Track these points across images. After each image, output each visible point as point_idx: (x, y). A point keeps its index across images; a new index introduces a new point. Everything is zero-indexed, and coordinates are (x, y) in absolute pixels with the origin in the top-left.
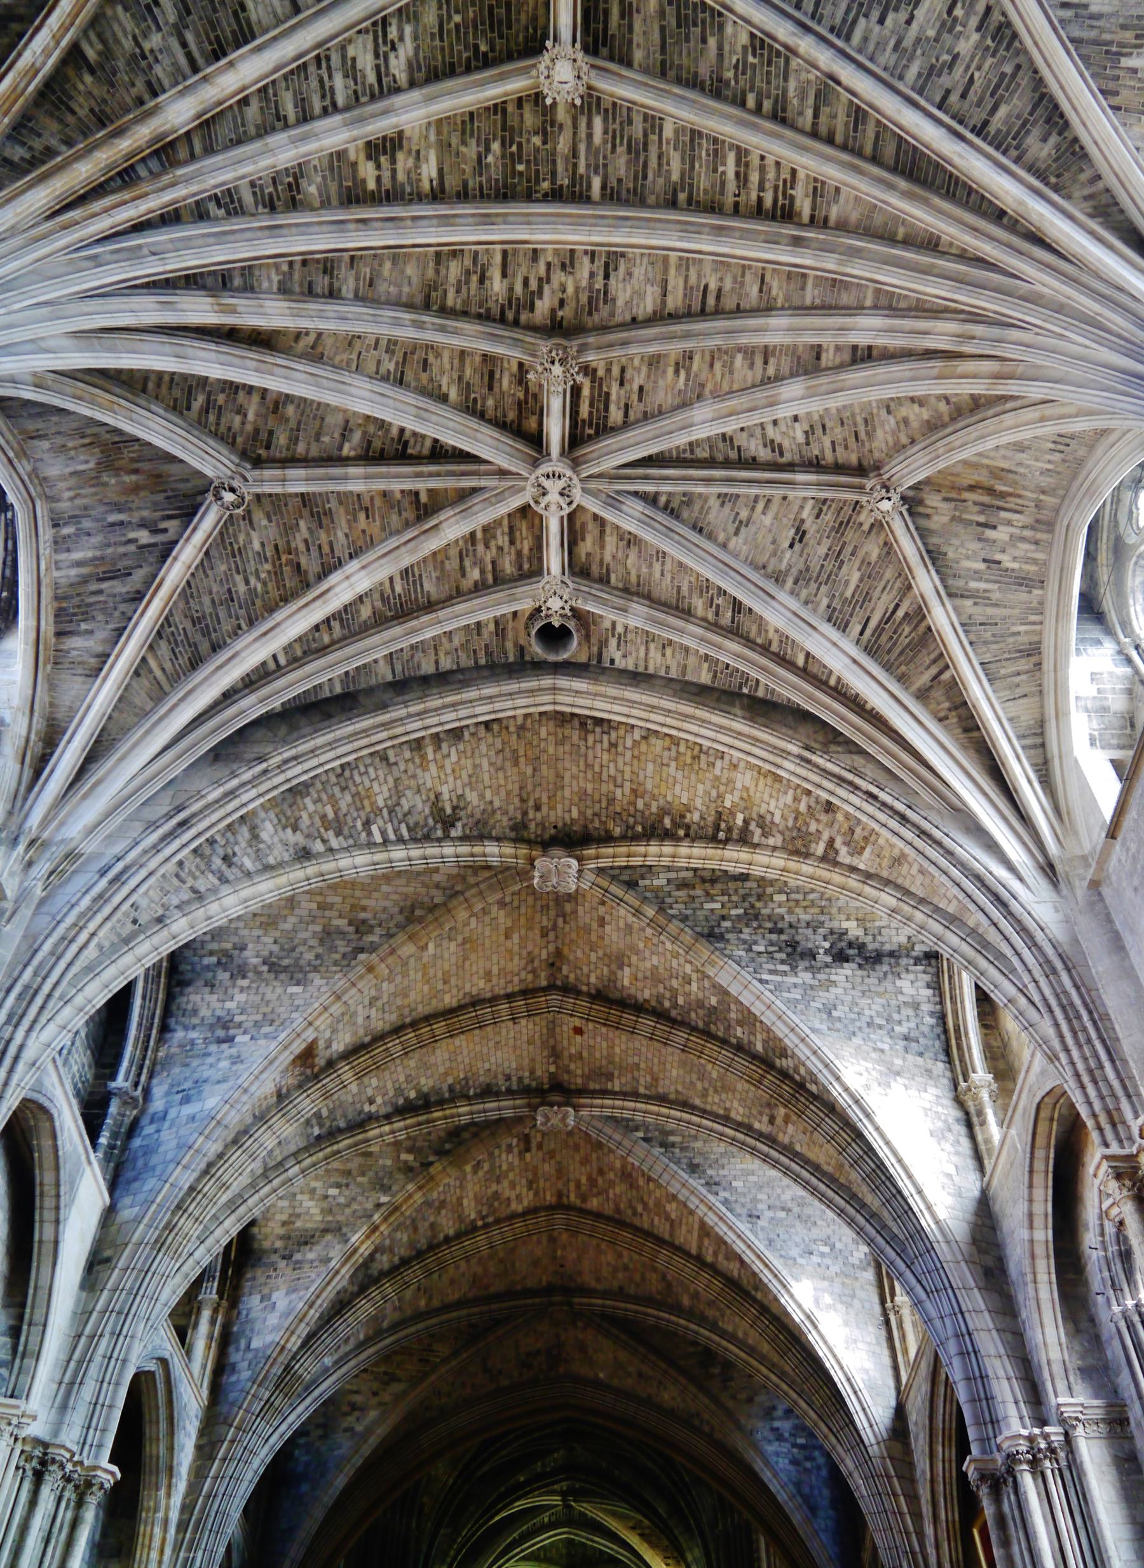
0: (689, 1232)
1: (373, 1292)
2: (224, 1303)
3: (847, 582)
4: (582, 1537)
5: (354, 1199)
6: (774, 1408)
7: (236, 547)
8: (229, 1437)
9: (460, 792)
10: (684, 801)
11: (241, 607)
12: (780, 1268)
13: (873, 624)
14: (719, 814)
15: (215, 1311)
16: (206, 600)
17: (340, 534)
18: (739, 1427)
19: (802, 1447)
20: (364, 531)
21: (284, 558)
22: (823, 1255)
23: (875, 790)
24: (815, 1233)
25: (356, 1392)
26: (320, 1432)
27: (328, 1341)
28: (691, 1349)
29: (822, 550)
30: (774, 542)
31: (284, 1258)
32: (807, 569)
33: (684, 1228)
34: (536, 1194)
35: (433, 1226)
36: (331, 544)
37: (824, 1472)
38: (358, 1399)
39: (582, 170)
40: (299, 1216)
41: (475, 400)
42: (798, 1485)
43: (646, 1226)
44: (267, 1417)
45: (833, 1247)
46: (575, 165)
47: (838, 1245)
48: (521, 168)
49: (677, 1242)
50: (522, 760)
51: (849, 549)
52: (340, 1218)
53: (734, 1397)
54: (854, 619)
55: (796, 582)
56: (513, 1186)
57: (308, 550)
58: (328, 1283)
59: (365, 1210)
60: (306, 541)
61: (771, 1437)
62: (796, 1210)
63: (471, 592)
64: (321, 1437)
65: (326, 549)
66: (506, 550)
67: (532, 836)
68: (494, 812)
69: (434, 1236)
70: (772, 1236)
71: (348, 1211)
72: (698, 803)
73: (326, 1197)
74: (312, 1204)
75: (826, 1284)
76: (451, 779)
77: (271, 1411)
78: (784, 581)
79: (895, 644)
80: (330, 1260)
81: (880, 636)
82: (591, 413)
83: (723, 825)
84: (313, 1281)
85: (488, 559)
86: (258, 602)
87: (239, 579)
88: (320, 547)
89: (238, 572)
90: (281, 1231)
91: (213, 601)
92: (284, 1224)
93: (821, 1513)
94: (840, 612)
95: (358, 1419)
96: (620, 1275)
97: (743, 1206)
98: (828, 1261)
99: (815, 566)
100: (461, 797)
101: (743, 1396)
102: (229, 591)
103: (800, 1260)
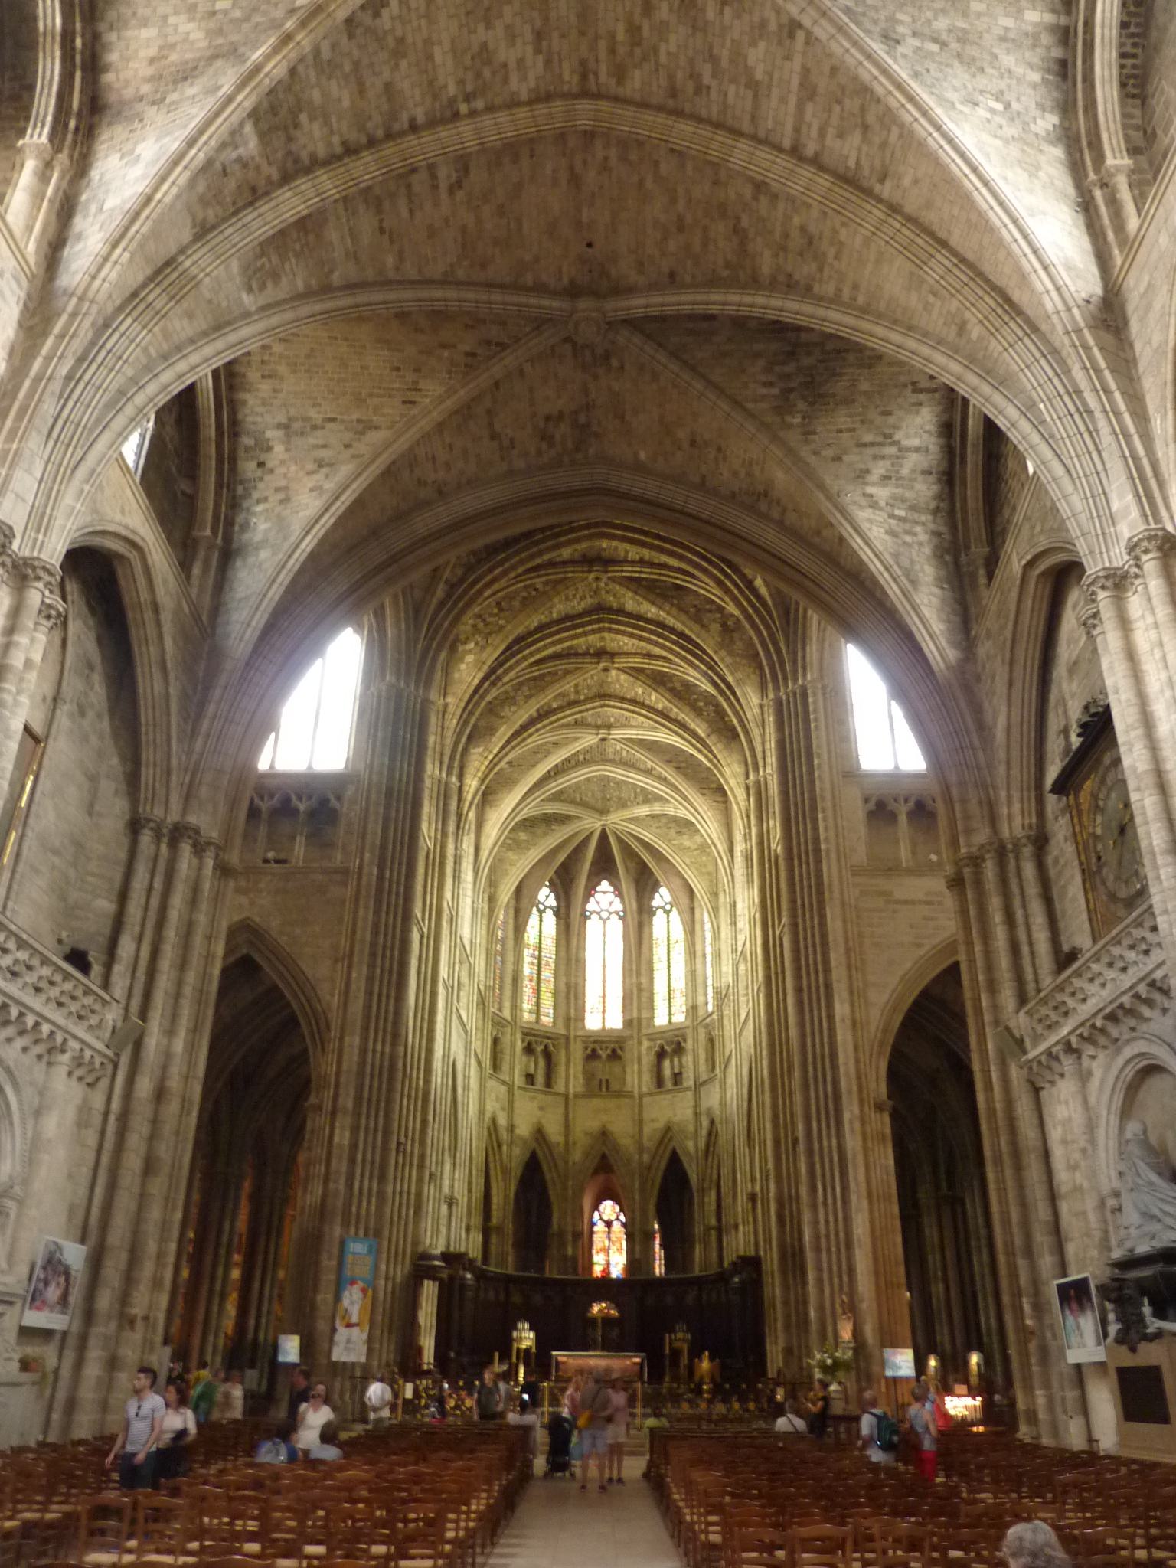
0: (783, 100)
1: (303, 184)
2: (63, 157)
4: (617, 773)
5: (255, 10)
6: (868, 471)
8: (70, 309)
12: (932, 104)
15: (48, 165)
18: (822, 487)
19: (900, 519)
22: (993, 111)
24: (982, 82)
25: (324, 446)
26: (281, 496)
27: (236, 238)
28: (764, 391)
31: (154, 103)
33: (774, 102)
34: (548, 63)
35: (388, 86)
37: (927, 550)
38: (324, 454)
40: (173, 46)
42: (896, 556)
43: (715, 112)
44: (145, 318)
45: (1008, 106)
47: (1015, 106)
49: (762, 134)
52: (235, 38)
53: (816, 453)
56: (512, 36)
58: (217, 114)
59: (273, 20)
61: (863, 502)
62: (954, 46)
64: (281, 502)
69: (393, 116)
70: (919, 68)
71: (246, 27)
73: (214, 13)
74: (191, 26)
75: (998, 143)
77: (150, 313)
80: (219, 88)
84: (194, 117)
90: (150, 71)
92: (152, 61)
93: (924, 589)
95: (327, 476)
96: (672, 246)
97: (875, 22)
98: (998, 119)
101: (829, 453)
103: (959, 106)
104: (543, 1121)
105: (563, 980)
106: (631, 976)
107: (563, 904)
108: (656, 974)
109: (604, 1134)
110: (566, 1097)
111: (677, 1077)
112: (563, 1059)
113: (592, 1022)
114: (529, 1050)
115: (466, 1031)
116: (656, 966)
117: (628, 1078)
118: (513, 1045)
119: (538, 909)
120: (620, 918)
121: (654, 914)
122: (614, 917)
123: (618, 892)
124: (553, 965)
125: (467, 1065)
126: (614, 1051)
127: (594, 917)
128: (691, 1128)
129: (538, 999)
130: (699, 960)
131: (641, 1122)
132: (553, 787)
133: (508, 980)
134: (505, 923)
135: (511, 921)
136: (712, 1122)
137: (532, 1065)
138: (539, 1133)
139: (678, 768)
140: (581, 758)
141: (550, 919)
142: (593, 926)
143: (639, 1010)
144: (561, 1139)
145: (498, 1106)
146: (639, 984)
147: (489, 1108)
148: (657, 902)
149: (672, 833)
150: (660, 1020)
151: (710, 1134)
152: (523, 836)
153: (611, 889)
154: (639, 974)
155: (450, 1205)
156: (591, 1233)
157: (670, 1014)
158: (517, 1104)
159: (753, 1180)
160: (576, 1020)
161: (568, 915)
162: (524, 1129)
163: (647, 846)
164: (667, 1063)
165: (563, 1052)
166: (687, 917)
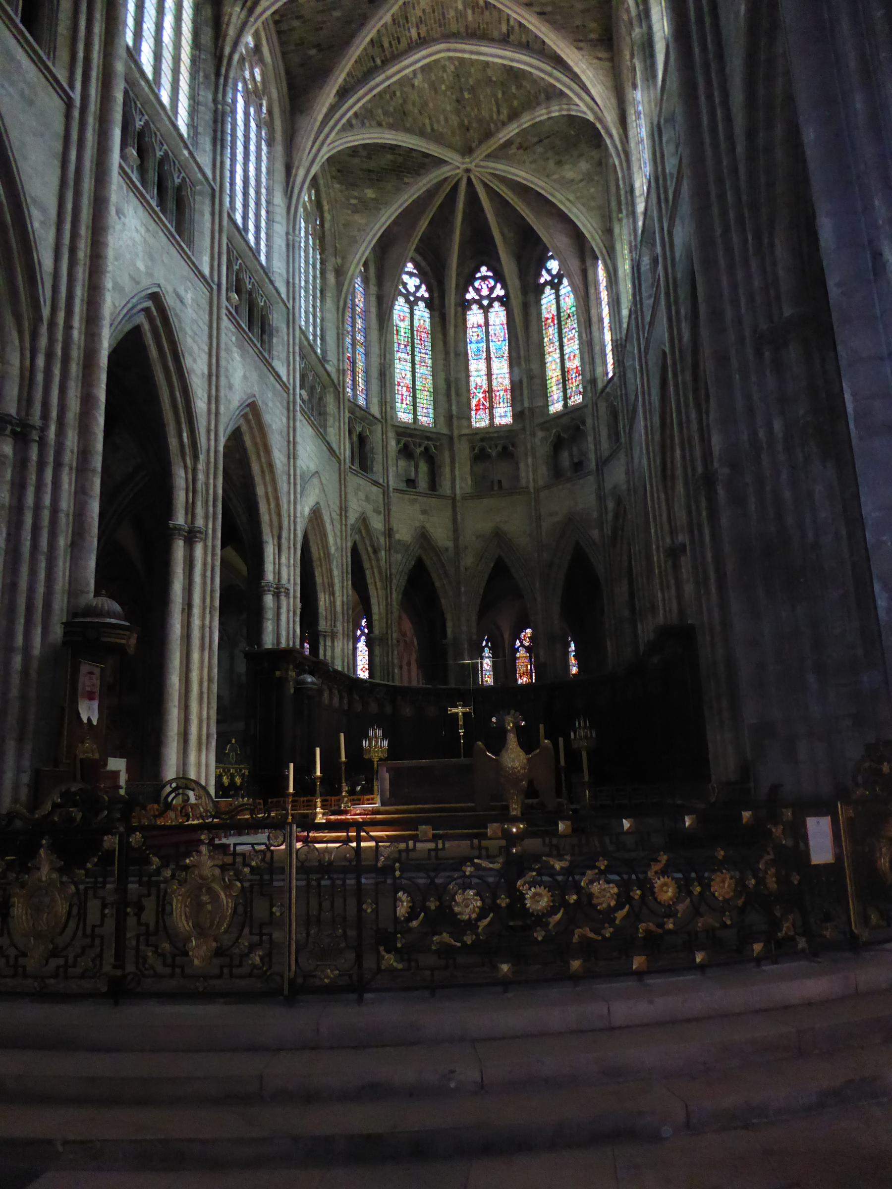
104: (427, 525)
105: (442, 376)
106: (519, 364)
107: (436, 295)
108: (548, 359)
109: (498, 535)
110: (454, 500)
111: (578, 466)
112: (447, 461)
113: (479, 421)
114: (406, 452)
115: (285, 386)
116: (548, 349)
117: (523, 474)
118: (385, 447)
119: (407, 301)
120: (503, 304)
121: (543, 292)
122: (496, 304)
123: (499, 277)
124: (429, 362)
125: (291, 429)
126: (505, 448)
127: (475, 307)
128: (595, 515)
129: (414, 397)
130: (595, 328)
131: (539, 518)
132: (382, 81)
133: (375, 373)
134: (366, 311)
135: (374, 310)
136: (619, 502)
137: (413, 469)
138: (423, 537)
139: (541, 14)
140: (414, 32)
141: (422, 313)
142: (475, 316)
143: (531, 399)
144: (450, 544)
145: (369, 508)
146: (530, 370)
147: (355, 507)
148: (545, 277)
149: (551, 164)
150: (556, 407)
151: (616, 517)
152: (370, 193)
153: (490, 274)
154: (528, 360)
155: (277, 595)
156: (515, 659)
157: (566, 398)
158: (394, 509)
159: (673, 532)
160: (458, 418)
161: (443, 305)
162: (404, 533)
163: (524, 191)
164: (565, 455)
165: (447, 454)
166: (578, 281)
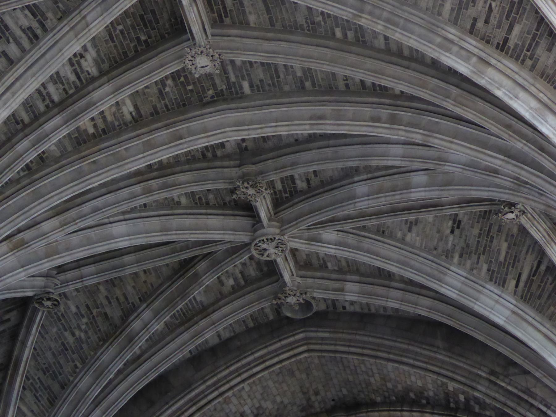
3: (499, 251)
7: (60, 314)
9: (257, 405)
10: (420, 384)
11: (74, 353)
13: (524, 277)
14: (447, 394)
16: (49, 355)
17: (129, 288)
20: (145, 282)
21: (95, 312)
23: (544, 409)
29: (476, 231)
30: (439, 231)
32: (468, 246)
36: (124, 295)
39: (233, 79)
41: (200, 198)
46: (227, 78)
48: (190, 87)
50: (297, 373)
51: (495, 228)
54: (509, 276)
55: (461, 256)
57: (110, 303)
60: (107, 297)
63: (231, 293)
65: (122, 299)
66: (248, 264)
67: (318, 410)
68: (285, 407)
72: (430, 386)
76: (249, 401)
78: (452, 257)
79: (543, 290)
81: (531, 285)
82: (283, 187)
83: (452, 400)
85: (237, 271)
86: (85, 346)
87: (67, 334)
88: (117, 298)
89: (66, 330)
91: (54, 354)
94: (498, 273)
99: (473, 242)
100: (257, 409)
102: (63, 344)
